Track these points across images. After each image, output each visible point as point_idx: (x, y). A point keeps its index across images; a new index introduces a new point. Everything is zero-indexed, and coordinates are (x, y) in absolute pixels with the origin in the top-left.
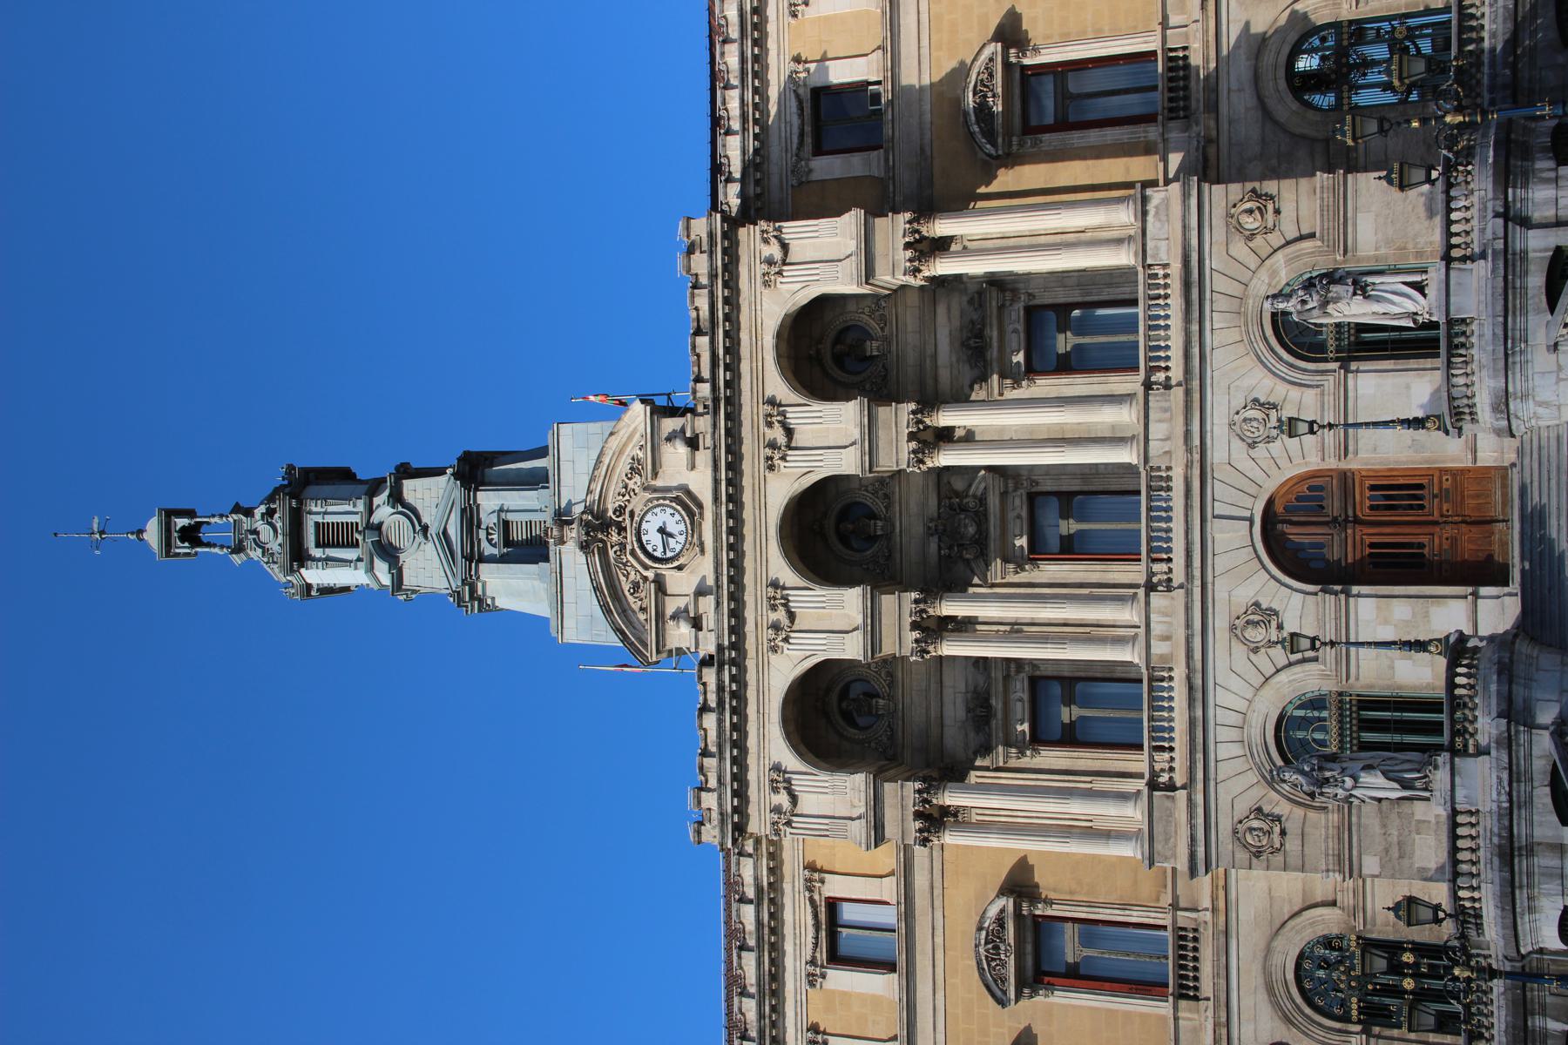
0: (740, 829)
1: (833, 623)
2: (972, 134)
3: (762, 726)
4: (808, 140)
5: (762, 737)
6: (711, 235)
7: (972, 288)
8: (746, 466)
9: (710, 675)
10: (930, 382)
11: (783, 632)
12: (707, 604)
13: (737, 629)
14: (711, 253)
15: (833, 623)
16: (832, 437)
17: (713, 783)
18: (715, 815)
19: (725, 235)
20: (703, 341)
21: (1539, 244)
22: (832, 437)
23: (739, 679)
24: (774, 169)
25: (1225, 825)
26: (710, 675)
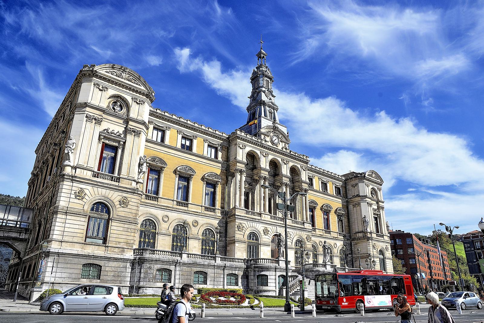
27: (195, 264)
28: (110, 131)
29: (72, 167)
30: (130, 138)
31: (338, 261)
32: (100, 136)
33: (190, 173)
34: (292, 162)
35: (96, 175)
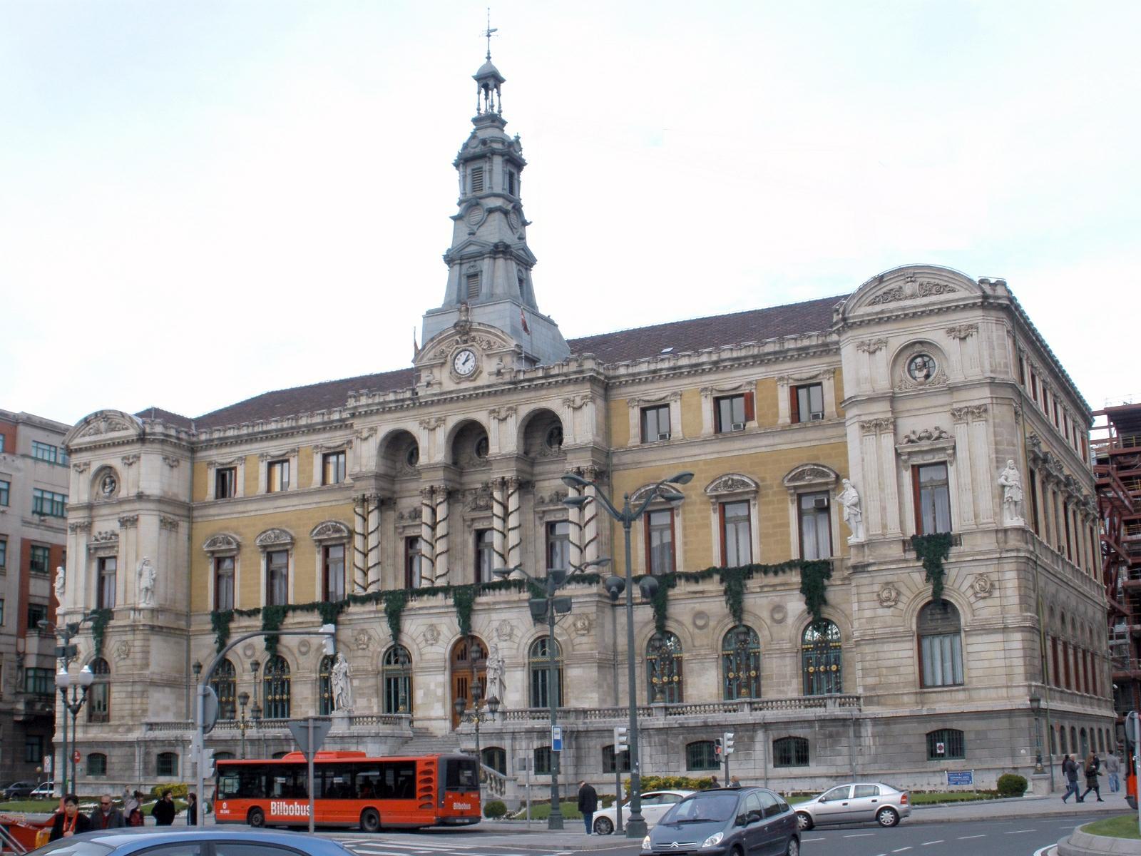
0: (353, 415)
1: (433, 448)
2: (639, 489)
3: (393, 420)
4: (647, 405)
5: (388, 421)
6: (582, 372)
8: (492, 400)
9: (408, 394)
10: (542, 477)
11: (425, 424)
12: (436, 390)
14: (575, 373)
16: (504, 439)
17: (370, 401)
18: (358, 404)
19: (584, 378)
20: (540, 374)
21: (506, 744)
22: (504, 439)
24: (635, 388)
25: (366, 626)
26: (408, 394)
28: (99, 537)
31: (788, 668)
32: (89, 549)
34: (527, 402)
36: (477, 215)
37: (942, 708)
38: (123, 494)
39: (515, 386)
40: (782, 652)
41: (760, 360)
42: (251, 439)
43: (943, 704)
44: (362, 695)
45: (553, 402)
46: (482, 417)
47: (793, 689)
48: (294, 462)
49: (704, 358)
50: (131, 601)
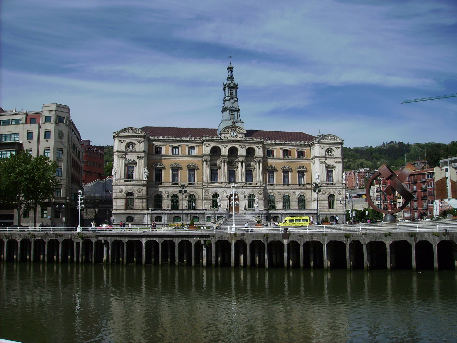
1: (225, 151)
7: (255, 166)
12: (226, 139)
13: (224, 142)
15: (225, 151)
16: (242, 152)
21: (260, 215)
22: (242, 152)
23: (219, 142)
27: (174, 214)
29: (116, 180)
30: (138, 161)
33: (178, 166)
35: (125, 181)
36: (232, 101)
37: (332, 213)
38: (137, 150)
39: (246, 142)
40: (295, 201)
41: (293, 145)
42: (168, 141)
43: (332, 212)
44: (207, 204)
45: (254, 146)
46: (237, 146)
47: (297, 208)
48: (180, 148)
49: (281, 142)
50: (141, 178)
